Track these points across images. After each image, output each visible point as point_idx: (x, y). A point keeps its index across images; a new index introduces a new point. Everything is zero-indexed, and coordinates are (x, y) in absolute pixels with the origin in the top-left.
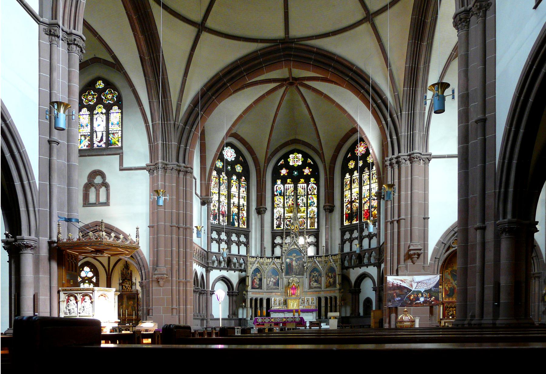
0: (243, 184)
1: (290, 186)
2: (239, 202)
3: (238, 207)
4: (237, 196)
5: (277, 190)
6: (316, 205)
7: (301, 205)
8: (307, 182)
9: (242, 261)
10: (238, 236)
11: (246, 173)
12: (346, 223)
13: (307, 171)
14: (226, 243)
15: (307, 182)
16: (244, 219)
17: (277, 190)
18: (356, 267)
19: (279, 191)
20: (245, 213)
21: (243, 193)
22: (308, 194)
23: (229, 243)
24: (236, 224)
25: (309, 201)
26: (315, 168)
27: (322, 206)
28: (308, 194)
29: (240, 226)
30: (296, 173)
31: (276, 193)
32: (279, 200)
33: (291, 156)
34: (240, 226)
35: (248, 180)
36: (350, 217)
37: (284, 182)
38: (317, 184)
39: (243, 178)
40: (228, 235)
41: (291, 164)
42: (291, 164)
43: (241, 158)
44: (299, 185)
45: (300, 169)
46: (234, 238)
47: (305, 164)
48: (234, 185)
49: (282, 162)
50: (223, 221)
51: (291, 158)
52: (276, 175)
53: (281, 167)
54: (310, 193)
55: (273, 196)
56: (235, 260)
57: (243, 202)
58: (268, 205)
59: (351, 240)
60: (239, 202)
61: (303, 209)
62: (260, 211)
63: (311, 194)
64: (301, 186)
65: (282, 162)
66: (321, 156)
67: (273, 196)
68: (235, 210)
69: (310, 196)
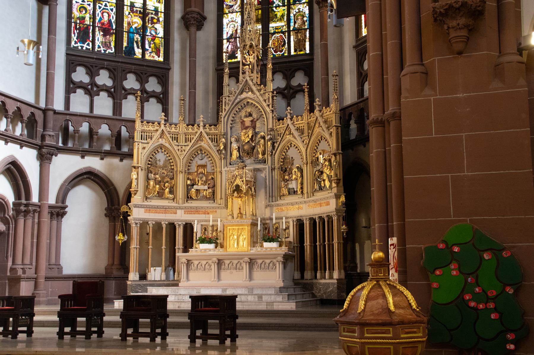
3: (144, 13)
10: (142, 79)
16: (157, 41)
20: (160, 29)
23: (117, 94)
24: (138, 52)
29: (147, 57)
34: (147, 57)
40: (117, 76)
46: (131, 82)
50: (107, 45)
68: (137, 22)
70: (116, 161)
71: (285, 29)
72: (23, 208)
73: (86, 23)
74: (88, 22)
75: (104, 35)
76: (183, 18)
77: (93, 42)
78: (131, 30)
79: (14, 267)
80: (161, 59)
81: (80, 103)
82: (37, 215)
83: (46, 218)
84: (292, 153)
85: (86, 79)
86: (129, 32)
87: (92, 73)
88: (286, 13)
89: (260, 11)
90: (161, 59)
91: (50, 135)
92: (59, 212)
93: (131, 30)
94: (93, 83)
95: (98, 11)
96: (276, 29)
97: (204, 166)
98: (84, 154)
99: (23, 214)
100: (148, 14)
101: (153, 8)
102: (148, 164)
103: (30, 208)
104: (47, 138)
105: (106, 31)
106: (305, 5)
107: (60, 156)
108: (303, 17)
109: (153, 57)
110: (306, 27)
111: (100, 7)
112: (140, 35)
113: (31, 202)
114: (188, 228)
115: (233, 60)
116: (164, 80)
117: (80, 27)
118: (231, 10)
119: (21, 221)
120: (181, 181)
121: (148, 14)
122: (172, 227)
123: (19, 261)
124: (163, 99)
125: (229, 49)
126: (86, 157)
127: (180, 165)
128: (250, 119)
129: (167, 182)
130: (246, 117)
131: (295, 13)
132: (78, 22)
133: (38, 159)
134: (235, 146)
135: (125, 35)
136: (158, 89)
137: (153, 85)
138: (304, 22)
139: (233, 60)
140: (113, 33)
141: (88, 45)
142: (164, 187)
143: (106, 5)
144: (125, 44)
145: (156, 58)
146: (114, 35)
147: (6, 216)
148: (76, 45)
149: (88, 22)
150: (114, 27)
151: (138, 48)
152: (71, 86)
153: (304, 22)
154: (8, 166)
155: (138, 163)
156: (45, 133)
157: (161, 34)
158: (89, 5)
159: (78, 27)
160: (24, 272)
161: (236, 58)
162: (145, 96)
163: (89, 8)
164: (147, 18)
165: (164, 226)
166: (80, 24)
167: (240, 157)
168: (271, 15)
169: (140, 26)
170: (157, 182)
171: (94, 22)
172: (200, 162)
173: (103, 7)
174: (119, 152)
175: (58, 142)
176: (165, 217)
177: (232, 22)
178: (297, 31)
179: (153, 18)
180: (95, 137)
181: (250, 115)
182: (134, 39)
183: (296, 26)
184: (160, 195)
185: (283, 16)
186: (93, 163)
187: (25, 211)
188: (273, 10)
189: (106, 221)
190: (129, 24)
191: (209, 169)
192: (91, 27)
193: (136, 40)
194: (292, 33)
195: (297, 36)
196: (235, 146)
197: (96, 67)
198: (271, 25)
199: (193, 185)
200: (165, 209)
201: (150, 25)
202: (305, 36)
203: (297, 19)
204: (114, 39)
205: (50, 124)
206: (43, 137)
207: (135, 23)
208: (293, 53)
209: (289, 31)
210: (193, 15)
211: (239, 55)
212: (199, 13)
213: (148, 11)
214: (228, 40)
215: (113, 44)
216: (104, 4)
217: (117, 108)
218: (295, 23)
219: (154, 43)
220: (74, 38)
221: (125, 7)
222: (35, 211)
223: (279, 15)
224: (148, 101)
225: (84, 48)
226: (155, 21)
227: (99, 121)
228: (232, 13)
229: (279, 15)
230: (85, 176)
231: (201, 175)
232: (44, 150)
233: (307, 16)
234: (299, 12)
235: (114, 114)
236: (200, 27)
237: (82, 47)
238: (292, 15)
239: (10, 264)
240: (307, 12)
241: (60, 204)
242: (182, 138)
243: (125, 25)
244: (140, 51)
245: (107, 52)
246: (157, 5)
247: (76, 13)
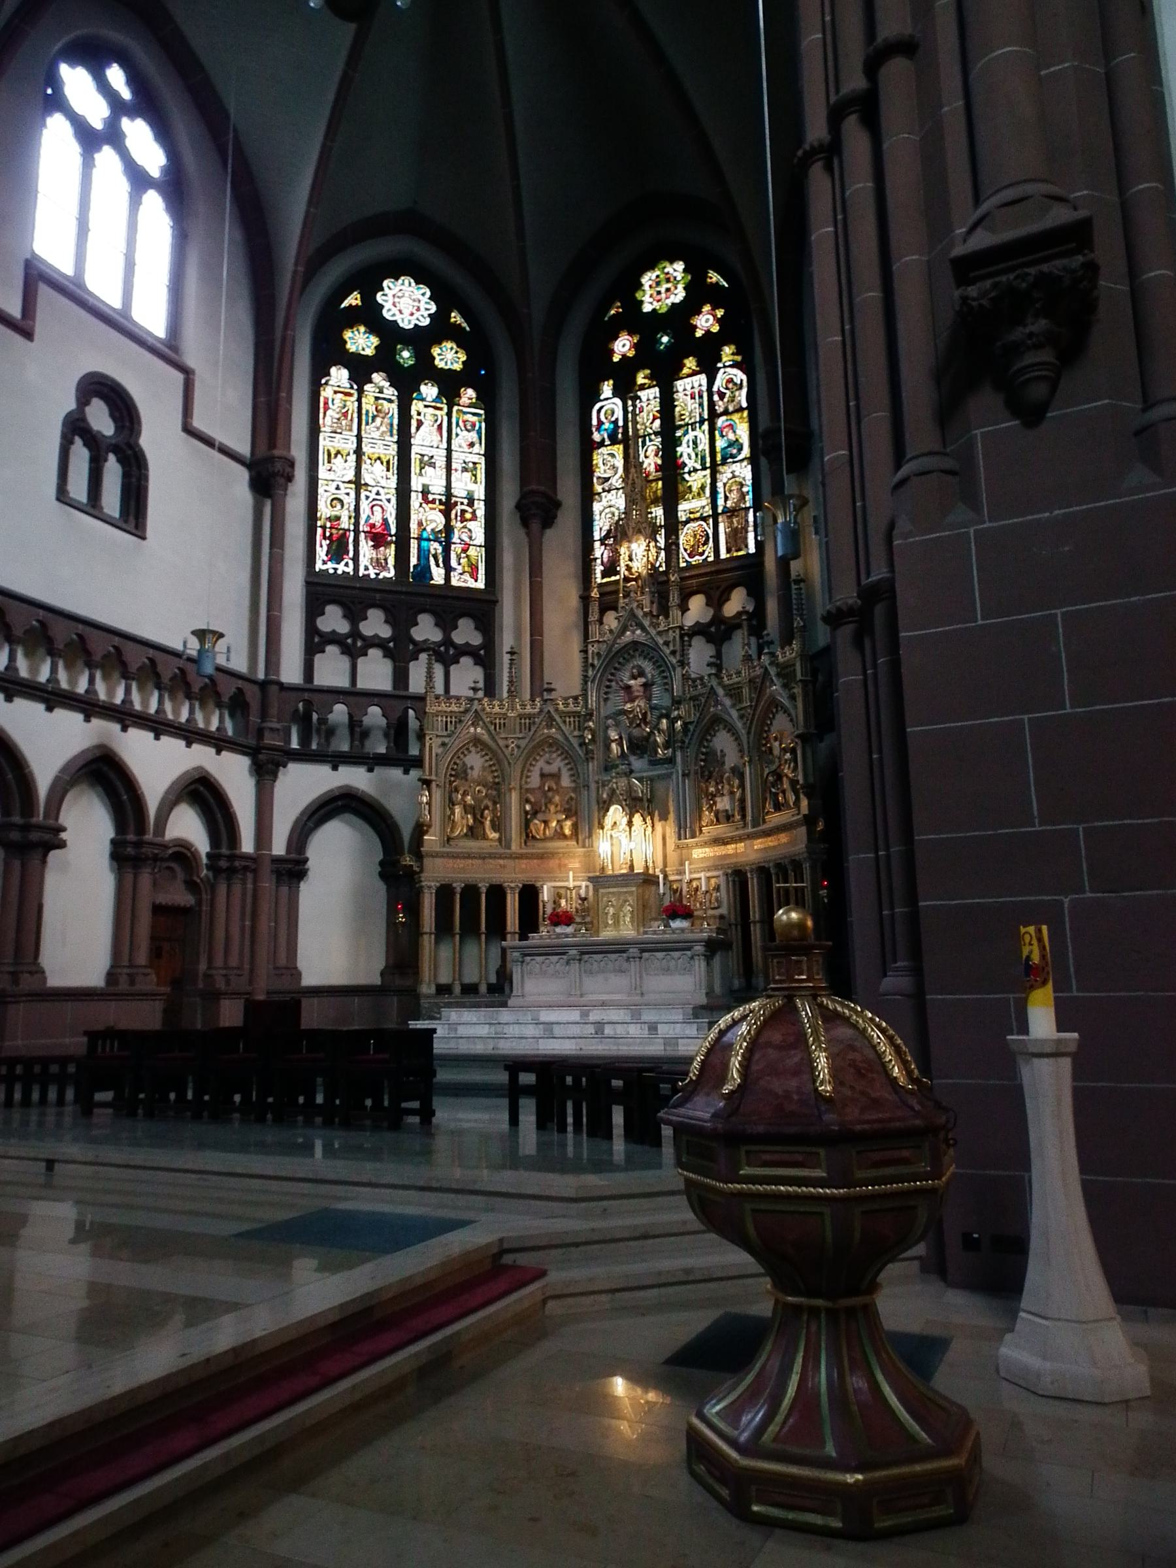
3: (448, 505)
4: (441, 461)
5: (600, 423)
6: (746, 452)
7: (691, 464)
10: (446, 624)
14: (388, 653)
16: (472, 552)
17: (600, 423)
19: (607, 425)
22: (713, 415)
23: (400, 652)
24: (438, 575)
25: (720, 444)
29: (455, 582)
30: (665, 339)
31: (597, 437)
32: (608, 462)
34: (455, 582)
35: (487, 400)
39: (471, 393)
40: (401, 620)
46: (426, 630)
48: (428, 422)
50: (380, 564)
51: (646, 287)
54: (720, 407)
55: (588, 447)
63: (726, 412)
64: (689, 386)
68: (436, 520)
69: (720, 422)
70: (396, 773)
71: (708, 511)
72: (223, 864)
73: (342, 526)
74: (345, 523)
75: (376, 547)
76: (518, 506)
77: (356, 559)
78: (425, 535)
79: (209, 972)
80: (481, 584)
81: (332, 670)
82: (250, 876)
83: (267, 883)
85: (343, 627)
86: (420, 539)
87: (355, 615)
88: (709, 481)
89: (660, 483)
90: (481, 584)
91: (272, 729)
92: (293, 869)
93: (425, 535)
94: (355, 633)
95: (365, 506)
96: (691, 513)
97: (556, 776)
98: (336, 761)
99: (224, 875)
100: (456, 503)
101: (464, 494)
102: (451, 775)
103: (237, 864)
104: (267, 734)
105: (379, 540)
106: (745, 463)
107: (292, 766)
108: (742, 485)
109: (465, 581)
110: (748, 505)
111: (367, 497)
112: (440, 543)
113: (237, 852)
114: (529, 894)
115: (613, 578)
117: (331, 534)
118: (606, 486)
119: (222, 889)
121: (456, 503)
122: (497, 893)
123: (219, 961)
124: (485, 656)
125: (605, 560)
126: (340, 768)
128: (642, 680)
129: (487, 808)
130: (634, 677)
131: (725, 480)
132: (328, 525)
133: (251, 774)
135: (414, 544)
136: (476, 639)
137: (466, 633)
138: (743, 496)
139: (613, 578)
140: (391, 542)
141: (347, 565)
142: (482, 816)
143: (378, 493)
144: (414, 561)
145: (471, 584)
146: (393, 546)
147: (195, 878)
148: (324, 567)
149: (345, 523)
150: (393, 531)
151: (438, 566)
152: (316, 640)
153: (743, 496)
154: (193, 787)
155: (430, 774)
156: (265, 725)
157: (479, 537)
158: (348, 494)
159: (328, 534)
160: (228, 983)
161: (618, 573)
163: (346, 499)
164: (453, 512)
165: (484, 890)
166: (331, 528)
167: (623, 755)
168: (681, 488)
169: (441, 527)
170: (467, 809)
171: (357, 524)
172: (548, 769)
173: (373, 496)
174: (401, 756)
175: (288, 741)
176: (483, 875)
178: (731, 512)
179: (463, 512)
180: (358, 729)
181: (641, 674)
182: (429, 551)
183: (729, 504)
185: (703, 488)
186: (355, 778)
187: (228, 869)
188: (684, 479)
189: (381, 887)
190: (420, 524)
191: (566, 781)
192: (352, 534)
193: (433, 552)
194: (720, 519)
195: (732, 523)
197: (361, 603)
198: (680, 507)
199: (535, 813)
201: (459, 525)
202: (747, 521)
203: (730, 491)
204: (393, 553)
205: (274, 711)
206: (260, 733)
207: (432, 521)
208: (723, 555)
209: (715, 516)
210: (536, 499)
212: (544, 494)
213: (454, 499)
214: (603, 541)
215: (391, 562)
216: (374, 490)
217: (401, 677)
218: (726, 498)
219: (467, 556)
220: (321, 553)
221: (413, 495)
222: (246, 868)
223: (695, 487)
224: (458, 662)
225: (340, 572)
226: (468, 516)
227: (364, 700)
228: (609, 491)
229: (695, 487)
230: (340, 803)
231: (550, 794)
232: (261, 756)
233: (749, 483)
234: (734, 477)
235: (395, 687)
236: (548, 520)
237: (336, 569)
238: (720, 485)
239: (203, 966)
240: (749, 476)
241: (293, 856)
243: (413, 526)
244: (442, 571)
245: (381, 577)
246: (472, 487)
247: (324, 510)
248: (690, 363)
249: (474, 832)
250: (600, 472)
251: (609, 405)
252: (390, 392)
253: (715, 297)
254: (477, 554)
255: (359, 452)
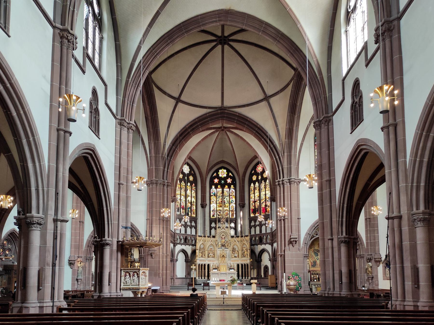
0: (194, 188)
1: (220, 190)
2: (191, 200)
3: (191, 203)
4: (190, 196)
6: (234, 202)
7: (226, 202)
8: (229, 187)
9: (193, 238)
11: (195, 181)
12: (252, 215)
13: (229, 181)
14: (184, 227)
15: (229, 187)
18: (259, 244)
20: (194, 207)
21: (194, 195)
22: (230, 196)
24: (190, 214)
25: (231, 200)
26: (233, 178)
27: (238, 203)
28: (230, 196)
31: (212, 194)
32: (213, 198)
33: (220, 171)
35: (196, 186)
36: (254, 211)
37: (216, 188)
38: (235, 189)
41: (220, 176)
42: (220, 176)
43: (192, 172)
44: (225, 189)
45: (225, 179)
47: (228, 176)
49: (215, 174)
52: (212, 183)
53: (215, 178)
55: (210, 196)
56: (189, 238)
57: (194, 200)
58: (208, 202)
59: (255, 226)
60: (191, 200)
61: (227, 205)
62: (203, 206)
64: (226, 189)
65: (215, 174)
66: (237, 172)
67: (210, 196)
68: (190, 205)
69: (231, 197)
80: (195, 216)
84: (235, 247)
98: (181, 244)
116: (196, 223)
120: (207, 253)
127: (206, 249)
134: (220, 244)
137: (193, 224)
149: (179, 206)
162: (191, 227)
176: (203, 263)
177: (213, 206)
178: (232, 211)
184: (202, 256)
191: (213, 249)
196: (220, 244)
200: (203, 261)
211: (215, 216)
242: (206, 241)
248: (227, 186)
249: (202, 256)
250: (212, 200)
251: (213, 189)
252: (184, 184)
253: (231, 177)
254: (195, 211)
255: (180, 194)
